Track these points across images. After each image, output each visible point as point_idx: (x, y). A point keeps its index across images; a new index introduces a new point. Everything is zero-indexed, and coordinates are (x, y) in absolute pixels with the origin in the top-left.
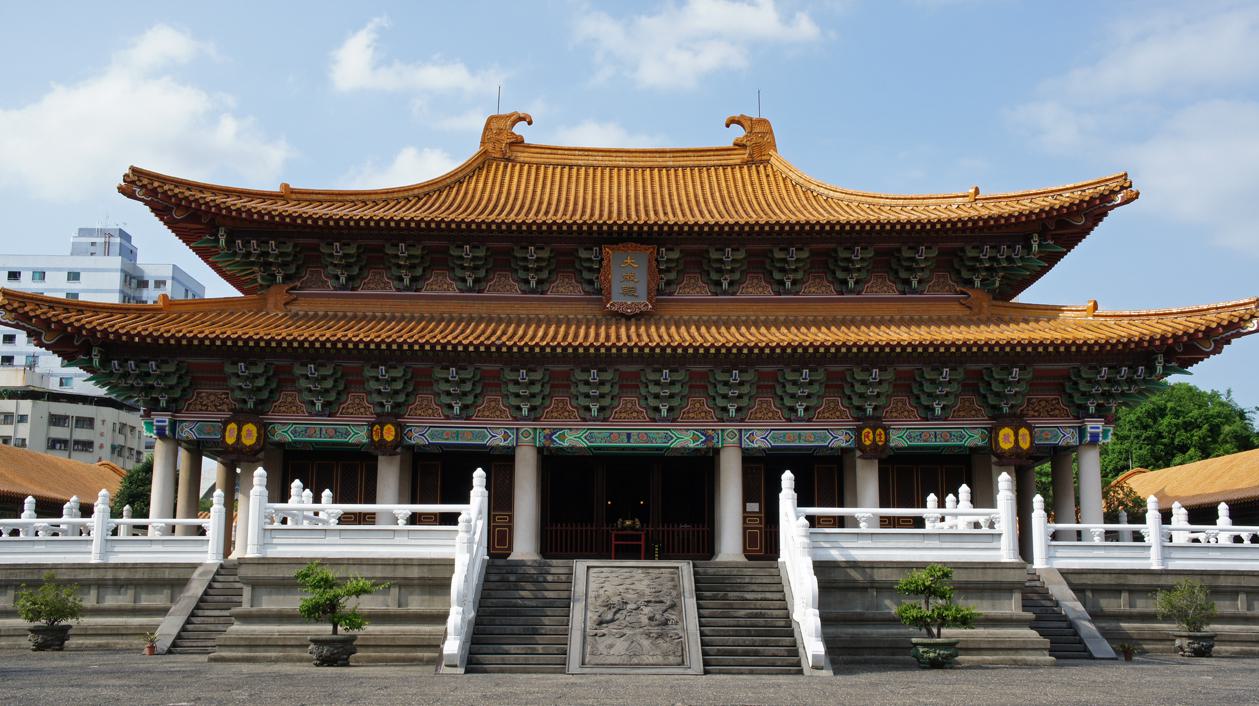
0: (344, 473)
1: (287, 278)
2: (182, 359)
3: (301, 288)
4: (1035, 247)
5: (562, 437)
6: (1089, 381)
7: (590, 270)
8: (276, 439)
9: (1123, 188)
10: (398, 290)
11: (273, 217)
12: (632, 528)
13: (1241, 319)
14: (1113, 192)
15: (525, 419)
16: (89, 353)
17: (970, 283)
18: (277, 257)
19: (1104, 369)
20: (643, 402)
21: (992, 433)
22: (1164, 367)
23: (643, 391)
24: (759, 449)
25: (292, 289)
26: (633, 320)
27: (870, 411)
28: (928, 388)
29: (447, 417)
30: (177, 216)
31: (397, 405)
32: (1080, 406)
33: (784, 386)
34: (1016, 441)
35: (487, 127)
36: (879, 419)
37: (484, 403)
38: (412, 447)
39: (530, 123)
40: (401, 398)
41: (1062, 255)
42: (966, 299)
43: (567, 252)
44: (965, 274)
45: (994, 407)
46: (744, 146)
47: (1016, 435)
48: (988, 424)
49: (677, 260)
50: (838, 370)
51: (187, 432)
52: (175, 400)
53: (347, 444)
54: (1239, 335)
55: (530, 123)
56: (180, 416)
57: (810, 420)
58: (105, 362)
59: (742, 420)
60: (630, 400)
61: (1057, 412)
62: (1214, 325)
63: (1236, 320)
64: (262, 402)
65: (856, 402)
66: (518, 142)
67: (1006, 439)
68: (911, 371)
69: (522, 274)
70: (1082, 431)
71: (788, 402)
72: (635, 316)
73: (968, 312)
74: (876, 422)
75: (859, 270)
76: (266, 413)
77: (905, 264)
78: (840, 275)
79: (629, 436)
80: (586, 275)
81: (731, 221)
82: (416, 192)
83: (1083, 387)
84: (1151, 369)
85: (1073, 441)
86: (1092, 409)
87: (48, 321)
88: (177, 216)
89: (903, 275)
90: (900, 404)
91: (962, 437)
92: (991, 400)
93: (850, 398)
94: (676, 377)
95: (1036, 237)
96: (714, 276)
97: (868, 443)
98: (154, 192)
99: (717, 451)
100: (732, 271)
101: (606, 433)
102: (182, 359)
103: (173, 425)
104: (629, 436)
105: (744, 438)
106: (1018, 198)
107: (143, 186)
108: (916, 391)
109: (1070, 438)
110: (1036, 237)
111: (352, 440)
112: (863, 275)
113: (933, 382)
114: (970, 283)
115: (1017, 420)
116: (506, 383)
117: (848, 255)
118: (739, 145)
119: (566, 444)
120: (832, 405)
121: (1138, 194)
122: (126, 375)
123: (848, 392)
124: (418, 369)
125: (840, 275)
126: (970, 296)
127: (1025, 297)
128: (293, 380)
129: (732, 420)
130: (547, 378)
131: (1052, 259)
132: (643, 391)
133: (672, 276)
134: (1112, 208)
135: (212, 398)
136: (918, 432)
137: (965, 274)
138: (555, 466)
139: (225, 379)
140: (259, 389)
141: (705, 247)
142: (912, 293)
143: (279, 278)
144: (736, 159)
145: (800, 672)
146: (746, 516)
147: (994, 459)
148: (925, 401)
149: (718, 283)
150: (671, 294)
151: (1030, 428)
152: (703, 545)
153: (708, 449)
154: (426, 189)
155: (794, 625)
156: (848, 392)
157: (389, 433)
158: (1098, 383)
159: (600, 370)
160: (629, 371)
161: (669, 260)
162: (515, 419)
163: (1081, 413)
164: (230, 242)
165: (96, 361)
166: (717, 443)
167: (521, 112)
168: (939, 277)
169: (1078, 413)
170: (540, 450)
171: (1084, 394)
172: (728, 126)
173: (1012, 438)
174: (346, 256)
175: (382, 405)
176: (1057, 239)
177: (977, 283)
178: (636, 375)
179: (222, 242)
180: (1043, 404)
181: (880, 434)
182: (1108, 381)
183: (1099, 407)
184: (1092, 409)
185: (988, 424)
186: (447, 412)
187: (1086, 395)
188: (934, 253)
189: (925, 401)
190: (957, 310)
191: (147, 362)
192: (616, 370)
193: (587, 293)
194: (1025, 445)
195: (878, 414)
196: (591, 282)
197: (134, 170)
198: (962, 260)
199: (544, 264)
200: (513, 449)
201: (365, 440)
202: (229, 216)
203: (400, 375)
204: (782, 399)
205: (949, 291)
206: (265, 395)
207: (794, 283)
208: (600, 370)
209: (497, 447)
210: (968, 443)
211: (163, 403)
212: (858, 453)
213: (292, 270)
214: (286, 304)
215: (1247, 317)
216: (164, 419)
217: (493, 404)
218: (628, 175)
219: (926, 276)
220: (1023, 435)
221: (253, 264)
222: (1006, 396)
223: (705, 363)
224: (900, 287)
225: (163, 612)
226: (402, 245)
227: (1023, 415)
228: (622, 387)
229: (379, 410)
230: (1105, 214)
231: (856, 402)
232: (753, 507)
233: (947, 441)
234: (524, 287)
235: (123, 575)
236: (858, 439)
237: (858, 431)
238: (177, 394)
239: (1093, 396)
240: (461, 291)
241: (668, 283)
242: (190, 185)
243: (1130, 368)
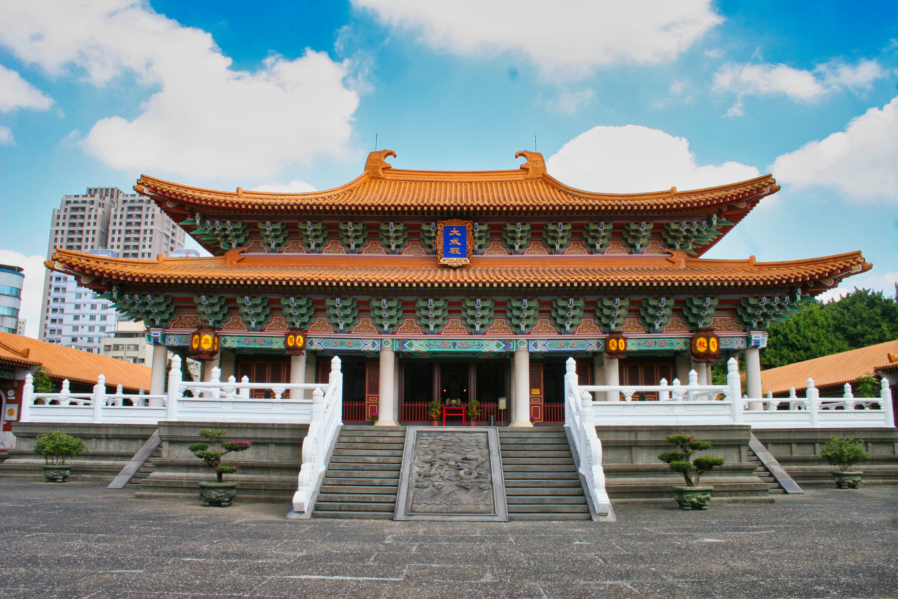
0: (262, 367)
1: (239, 245)
2: (168, 294)
3: (248, 252)
4: (715, 222)
5: (411, 345)
6: (753, 306)
7: (430, 238)
8: (227, 345)
10: (308, 252)
11: (227, 204)
12: (456, 405)
13: (852, 264)
15: (386, 333)
16: (110, 290)
17: (672, 247)
18: (232, 231)
19: (764, 298)
20: (464, 322)
21: (692, 341)
22: (802, 297)
23: (464, 314)
24: (541, 353)
25: (243, 252)
26: (458, 270)
27: (613, 327)
28: (651, 311)
29: (336, 332)
30: (170, 205)
31: (304, 324)
32: (746, 324)
33: (557, 311)
34: (708, 347)
35: (369, 159)
36: (620, 333)
37: (360, 322)
38: (315, 352)
39: (395, 156)
40: (306, 319)
41: (732, 227)
43: (415, 224)
44: (670, 241)
45: (692, 324)
46: (527, 170)
48: (690, 335)
49: (487, 231)
50: (594, 298)
51: (173, 341)
52: (166, 321)
53: (271, 350)
54: (847, 276)
55: (395, 156)
56: (168, 331)
57: (573, 333)
58: (120, 295)
59: (529, 333)
60: (455, 321)
62: (835, 268)
63: (848, 265)
64: (219, 322)
65: (604, 321)
66: (387, 168)
68: (641, 299)
69: (385, 241)
70: (748, 339)
71: (559, 321)
72: (459, 267)
73: (671, 265)
74: (617, 335)
75: (603, 237)
76: (221, 329)
77: (632, 234)
78: (590, 241)
79: (454, 344)
80: (427, 242)
81: (521, 204)
82: (323, 195)
83: (749, 310)
84: (793, 299)
85: (742, 346)
86: (755, 325)
87: (83, 269)
88: (170, 205)
89: (630, 241)
91: (672, 344)
92: (691, 320)
93: (600, 319)
94: (486, 304)
95: (715, 216)
96: (510, 242)
98: (155, 190)
99: (512, 354)
100: (521, 238)
101: (439, 343)
102: (168, 294)
103: (164, 336)
104: (454, 344)
105: (531, 345)
107: (149, 186)
108: (642, 314)
109: (738, 344)
110: (715, 216)
111: (275, 346)
112: (605, 241)
114: (672, 247)
115: (708, 333)
116: (373, 309)
118: (524, 169)
119: (413, 349)
122: (134, 304)
123: (598, 314)
124: (317, 296)
125: (590, 241)
128: (237, 308)
129: (522, 333)
130: (400, 306)
131: (725, 230)
132: (464, 314)
133: (483, 242)
134: (762, 197)
135: (188, 320)
136: (644, 341)
137: (670, 241)
138: (408, 365)
139: (195, 308)
140: (216, 313)
141: (503, 223)
143: (234, 246)
144: (521, 177)
145: (591, 519)
146: (532, 397)
147: (693, 358)
148: (648, 320)
149: (513, 247)
150: (482, 254)
151: (718, 338)
152: (505, 417)
153: (507, 353)
154: (329, 194)
155: (581, 477)
156: (598, 314)
157: (300, 340)
158: (760, 308)
159: (435, 300)
160: (456, 299)
161: (480, 231)
162: (380, 333)
163: (747, 327)
164: (203, 222)
165: (115, 296)
166: (512, 348)
167: (389, 149)
170: (397, 354)
171: (749, 315)
172: (516, 157)
173: (706, 345)
174: (274, 230)
175: (293, 324)
176: (728, 218)
177: (678, 247)
178: (459, 304)
179: (198, 222)
182: (766, 306)
183: (759, 323)
184: (755, 325)
185: (690, 335)
186: (335, 328)
188: (651, 226)
189: (648, 320)
191: (145, 295)
192: (446, 300)
193: (428, 253)
194: (713, 349)
195: (619, 329)
196: (430, 247)
197: (142, 176)
198: (668, 232)
199: (400, 234)
200: (378, 353)
201: (283, 347)
202: (201, 205)
203: (304, 303)
204: (555, 319)
205: (660, 252)
206: (220, 317)
207: (561, 246)
208: (435, 300)
209: (368, 352)
210: (676, 347)
211: (157, 323)
212: (605, 355)
213: (242, 240)
214: (238, 261)
215: (855, 263)
216: (157, 333)
217: (366, 323)
218: (456, 186)
221: (217, 235)
222: (701, 318)
223: (505, 295)
224: (629, 250)
225: (129, 456)
226: (309, 223)
227: (711, 330)
228: (450, 312)
229: (291, 326)
230: (758, 202)
231: (604, 321)
232: (537, 392)
234: (388, 250)
235: (111, 432)
236: (606, 345)
237: (606, 341)
238: (166, 316)
239: (756, 317)
240: (347, 253)
241: (480, 247)
242: (178, 187)
243: (780, 297)
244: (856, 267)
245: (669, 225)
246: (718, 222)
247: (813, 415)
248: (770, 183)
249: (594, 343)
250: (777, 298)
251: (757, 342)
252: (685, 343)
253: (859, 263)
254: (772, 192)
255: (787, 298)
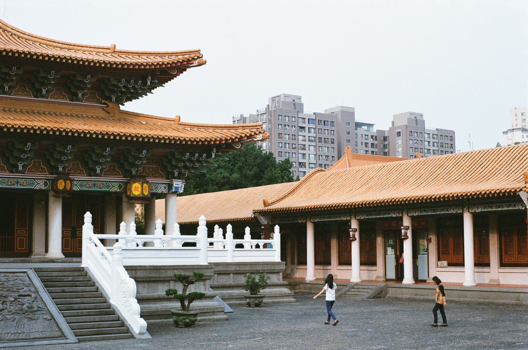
9: (199, 57)
13: (255, 133)
14: (194, 59)
22: (215, 155)
27: (61, 169)
42: (107, 107)
47: (142, 187)
61: (157, 175)
67: (136, 189)
70: (170, 186)
73: (107, 115)
74: (65, 176)
84: (209, 156)
85: (165, 191)
86: (176, 174)
89: (74, 90)
90: (76, 166)
91: (109, 186)
97: (61, 188)
106: (139, 54)
109: (162, 189)
113: (98, 155)
114: (110, 100)
117: (46, 75)
120: (37, 164)
121: (206, 62)
126: (108, 106)
127: (128, 106)
134: (190, 67)
142: (5, 94)
163: (170, 176)
168: (91, 93)
169: (169, 176)
173: (140, 189)
180: (151, 170)
181: (68, 184)
183: (180, 173)
184: (176, 174)
187: (176, 167)
190: (102, 114)
215: (258, 133)
219: (13, 85)
220: (145, 187)
222: (137, 166)
230: (185, 70)
233: (101, 188)
244: (258, 136)
245: (109, 80)
246: (151, 82)
247: (224, 250)
248: (199, 57)
249: (42, 183)
250: (197, 155)
251: (177, 188)
252: (120, 186)
253: (260, 133)
254: (200, 65)
255: (205, 155)
